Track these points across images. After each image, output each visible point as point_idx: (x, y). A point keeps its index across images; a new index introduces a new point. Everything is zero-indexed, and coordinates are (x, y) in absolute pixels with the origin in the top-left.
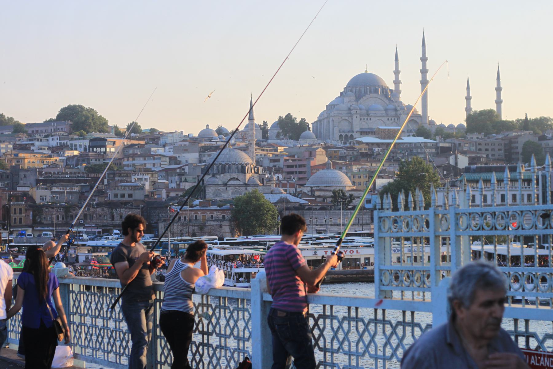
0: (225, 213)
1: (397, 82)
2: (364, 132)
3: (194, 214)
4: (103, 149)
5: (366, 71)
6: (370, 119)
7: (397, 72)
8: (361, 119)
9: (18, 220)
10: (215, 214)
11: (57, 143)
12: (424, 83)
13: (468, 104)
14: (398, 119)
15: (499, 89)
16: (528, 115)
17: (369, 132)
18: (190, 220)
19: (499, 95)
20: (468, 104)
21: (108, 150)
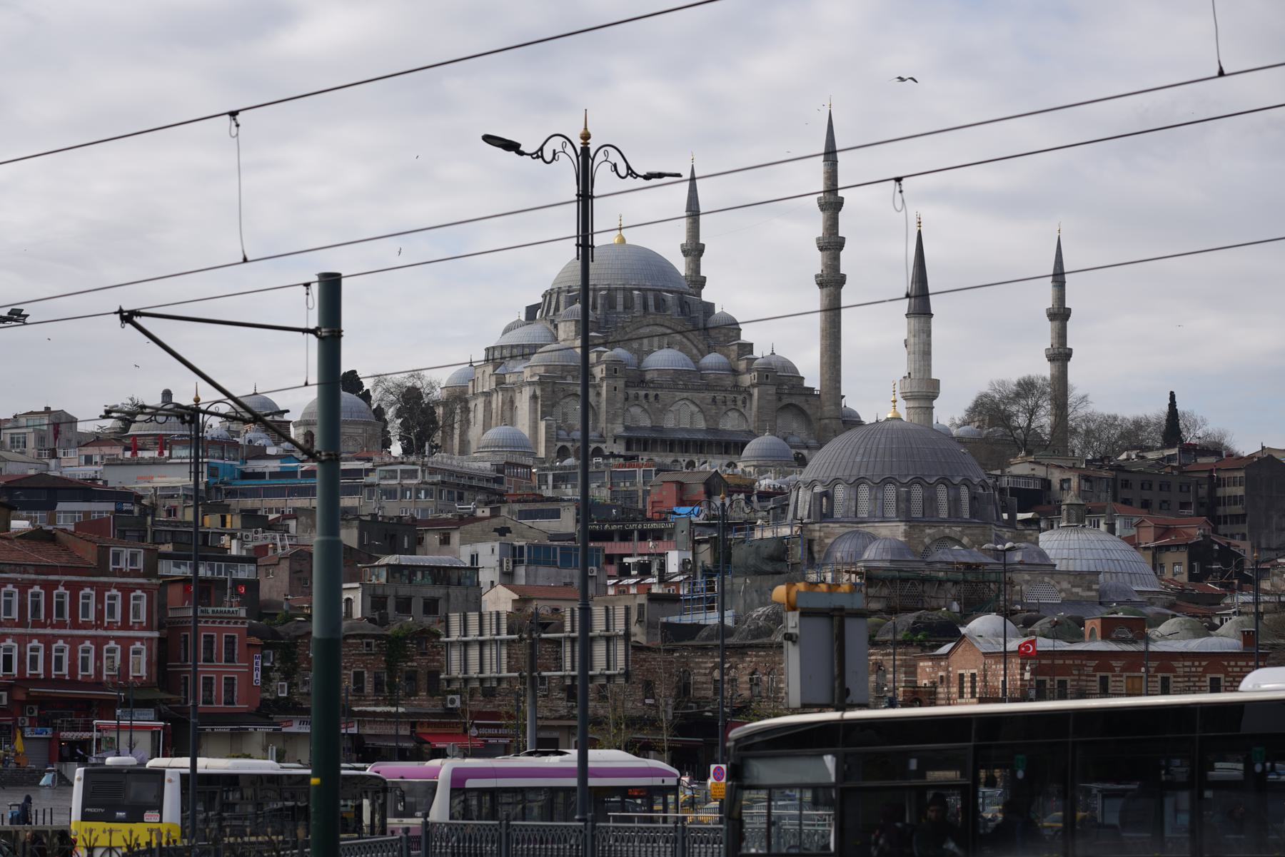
0: (1173, 670)
1: (700, 283)
2: (638, 440)
3: (1097, 669)
6: (656, 396)
8: (627, 399)
9: (219, 690)
10: (1180, 671)
12: (832, 281)
14: (744, 402)
16: (1177, 399)
17: (655, 441)
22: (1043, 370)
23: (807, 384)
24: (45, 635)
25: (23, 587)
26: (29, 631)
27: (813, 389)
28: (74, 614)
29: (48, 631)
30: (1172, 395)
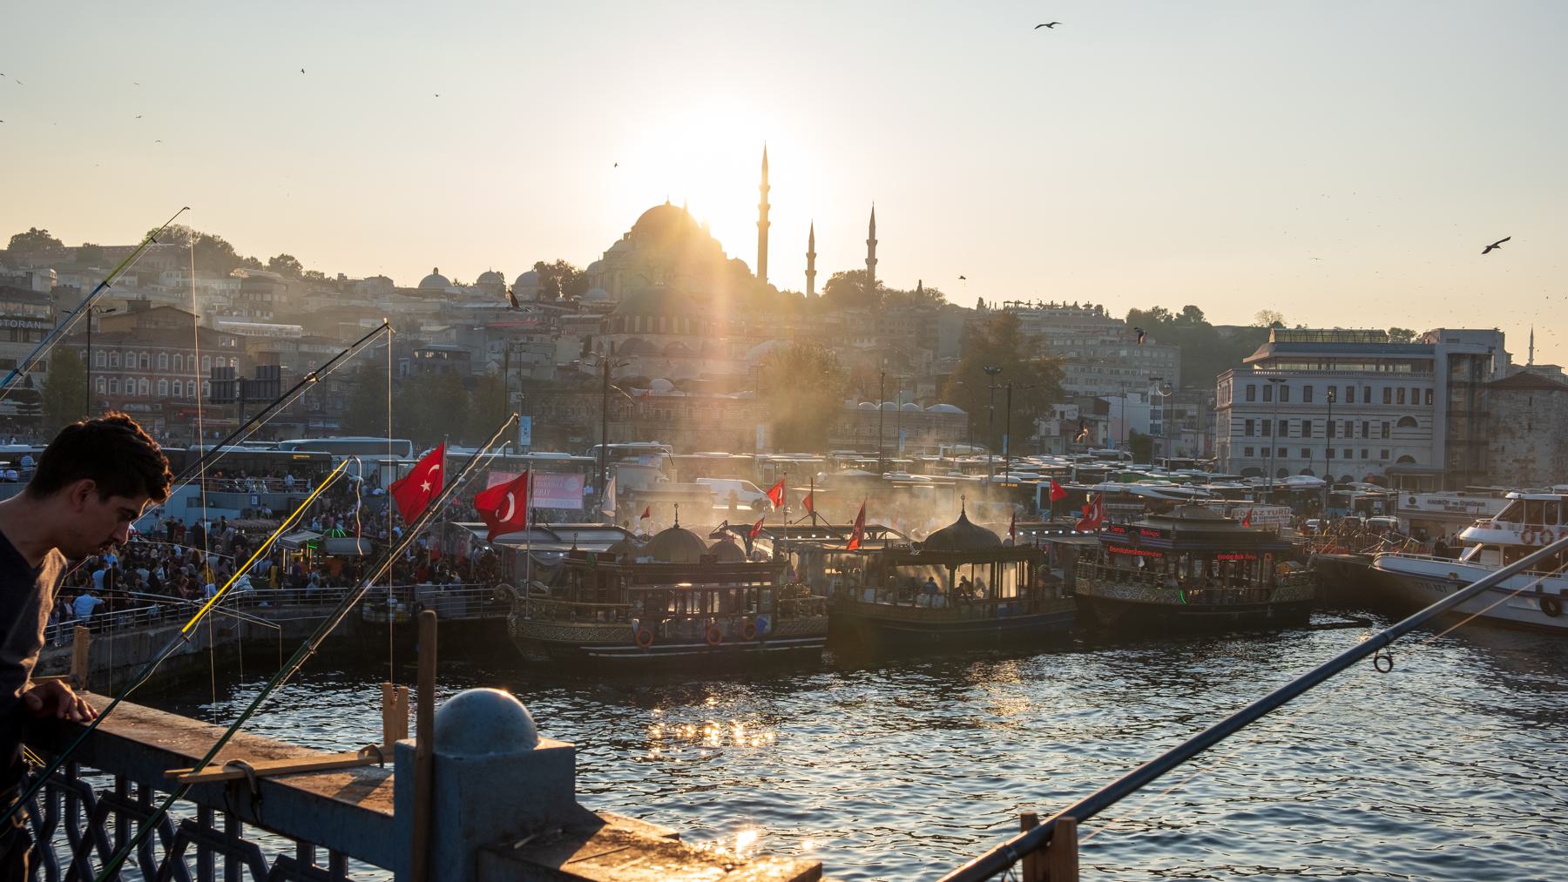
4: (268, 298)
5: (668, 202)
11: (178, 282)
15: (872, 243)
19: (872, 252)
21: (276, 298)
22: (864, 267)
23: (752, 272)
24: (183, 377)
25: (171, 354)
26: (175, 375)
27: (754, 275)
28: (185, 367)
29: (185, 375)
30: (920, 281)
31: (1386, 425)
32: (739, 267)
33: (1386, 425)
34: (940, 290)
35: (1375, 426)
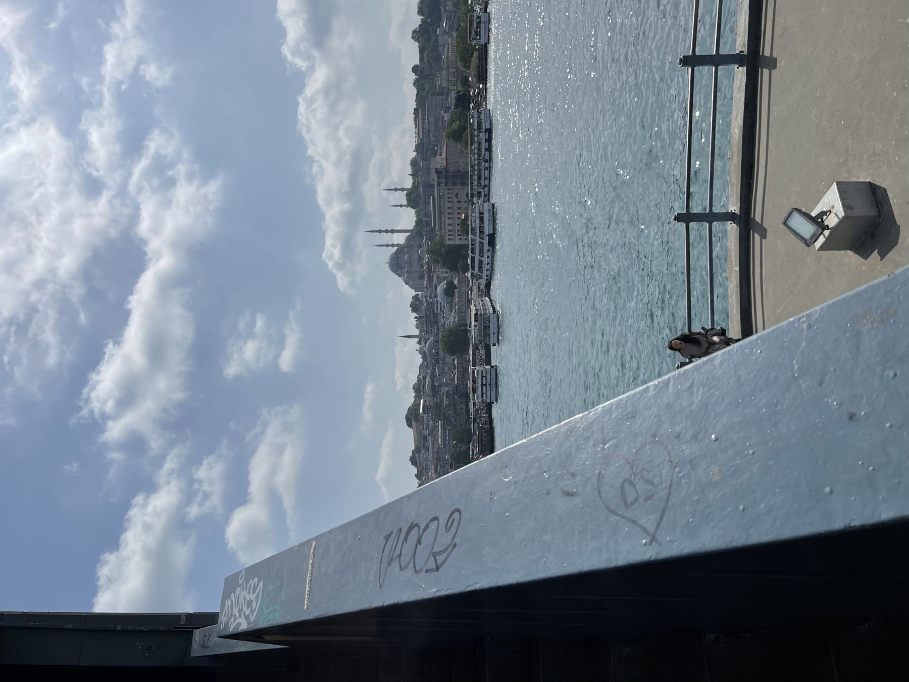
1: (393, 245)
7: (387, 245)
13: (404, 206)
18: (463, 375)
19: (399, 190)
20: (404, 206)
22: (405, 192)
31: (458, 202)
32: (408, 239)
33: (458, 202)
34: (411, 159)
35: (458, 205)
